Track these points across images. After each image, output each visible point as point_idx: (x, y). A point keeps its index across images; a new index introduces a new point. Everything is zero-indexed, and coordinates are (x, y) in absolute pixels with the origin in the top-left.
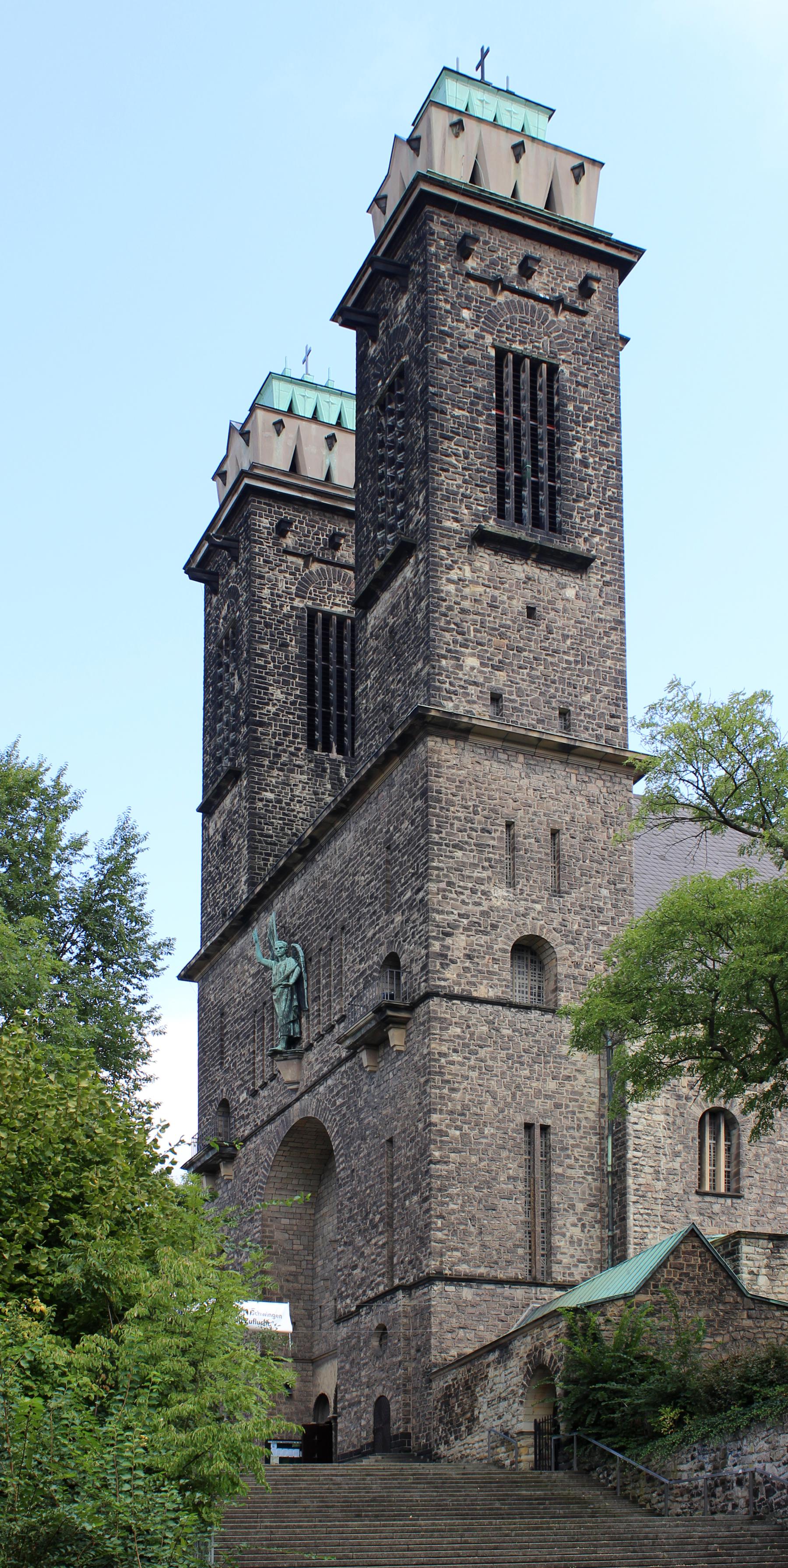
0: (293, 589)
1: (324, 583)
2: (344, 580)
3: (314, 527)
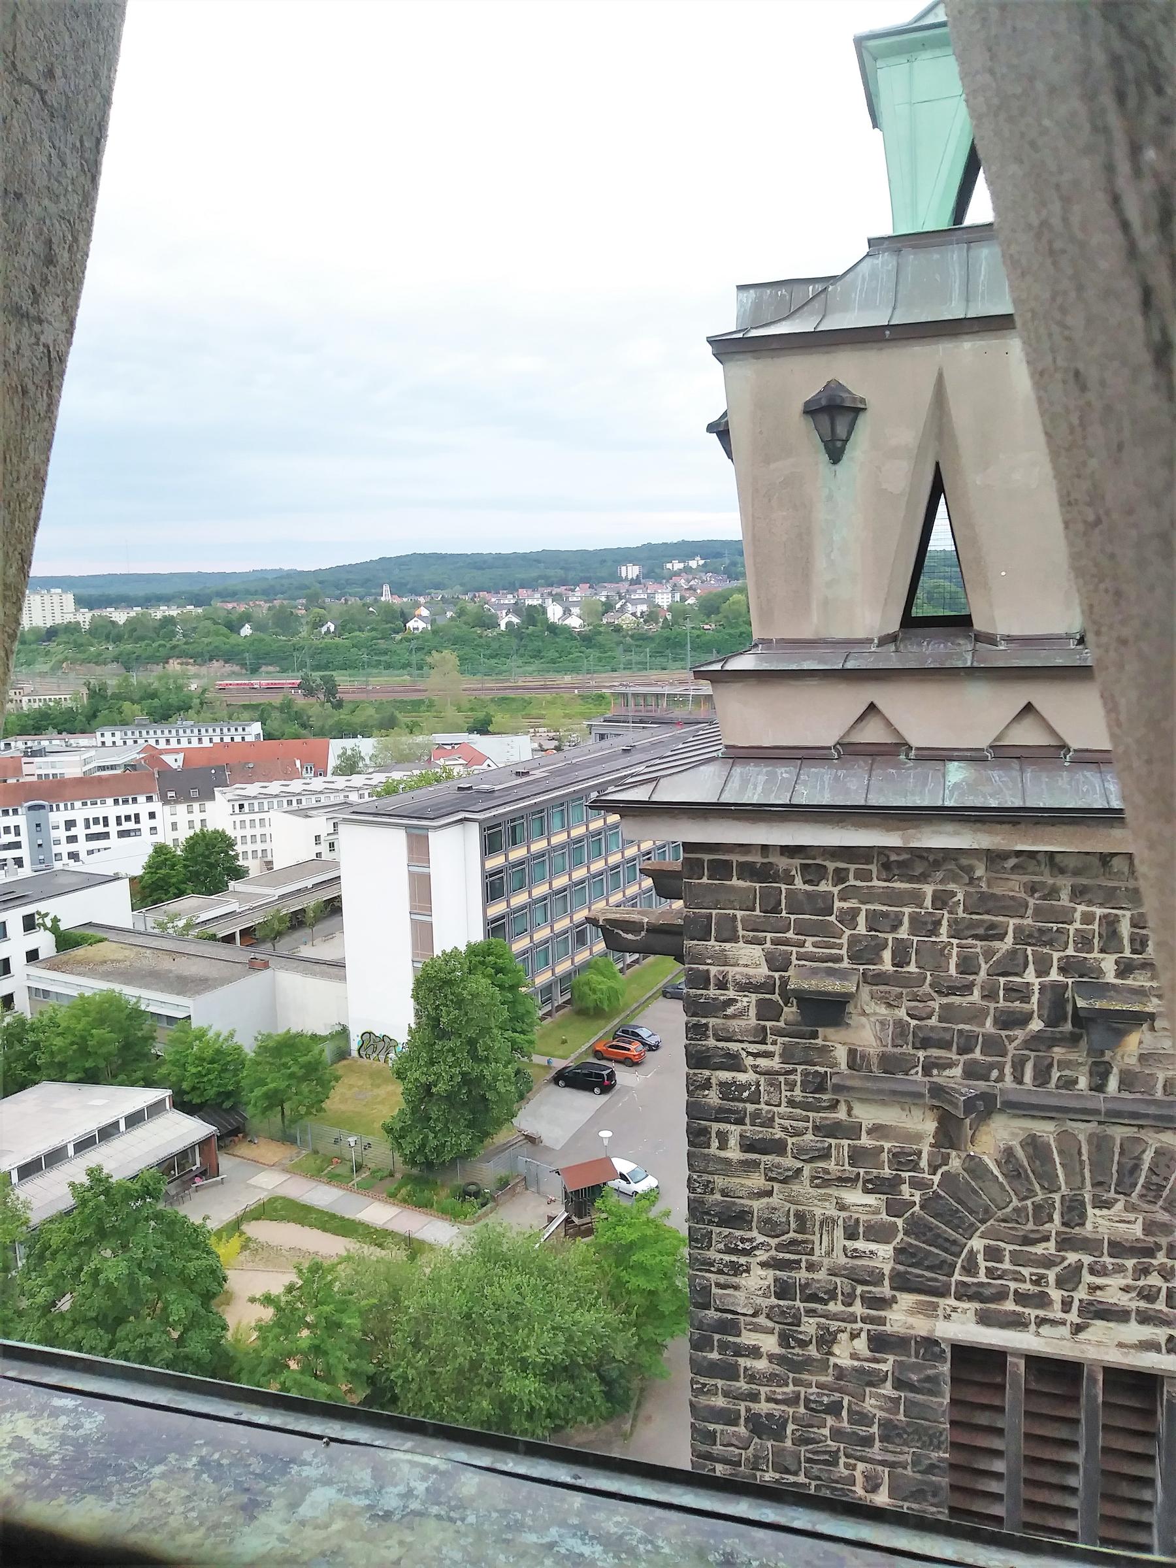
0: (883, 1255)
1: (1042, 1213)
3: (994, 933)
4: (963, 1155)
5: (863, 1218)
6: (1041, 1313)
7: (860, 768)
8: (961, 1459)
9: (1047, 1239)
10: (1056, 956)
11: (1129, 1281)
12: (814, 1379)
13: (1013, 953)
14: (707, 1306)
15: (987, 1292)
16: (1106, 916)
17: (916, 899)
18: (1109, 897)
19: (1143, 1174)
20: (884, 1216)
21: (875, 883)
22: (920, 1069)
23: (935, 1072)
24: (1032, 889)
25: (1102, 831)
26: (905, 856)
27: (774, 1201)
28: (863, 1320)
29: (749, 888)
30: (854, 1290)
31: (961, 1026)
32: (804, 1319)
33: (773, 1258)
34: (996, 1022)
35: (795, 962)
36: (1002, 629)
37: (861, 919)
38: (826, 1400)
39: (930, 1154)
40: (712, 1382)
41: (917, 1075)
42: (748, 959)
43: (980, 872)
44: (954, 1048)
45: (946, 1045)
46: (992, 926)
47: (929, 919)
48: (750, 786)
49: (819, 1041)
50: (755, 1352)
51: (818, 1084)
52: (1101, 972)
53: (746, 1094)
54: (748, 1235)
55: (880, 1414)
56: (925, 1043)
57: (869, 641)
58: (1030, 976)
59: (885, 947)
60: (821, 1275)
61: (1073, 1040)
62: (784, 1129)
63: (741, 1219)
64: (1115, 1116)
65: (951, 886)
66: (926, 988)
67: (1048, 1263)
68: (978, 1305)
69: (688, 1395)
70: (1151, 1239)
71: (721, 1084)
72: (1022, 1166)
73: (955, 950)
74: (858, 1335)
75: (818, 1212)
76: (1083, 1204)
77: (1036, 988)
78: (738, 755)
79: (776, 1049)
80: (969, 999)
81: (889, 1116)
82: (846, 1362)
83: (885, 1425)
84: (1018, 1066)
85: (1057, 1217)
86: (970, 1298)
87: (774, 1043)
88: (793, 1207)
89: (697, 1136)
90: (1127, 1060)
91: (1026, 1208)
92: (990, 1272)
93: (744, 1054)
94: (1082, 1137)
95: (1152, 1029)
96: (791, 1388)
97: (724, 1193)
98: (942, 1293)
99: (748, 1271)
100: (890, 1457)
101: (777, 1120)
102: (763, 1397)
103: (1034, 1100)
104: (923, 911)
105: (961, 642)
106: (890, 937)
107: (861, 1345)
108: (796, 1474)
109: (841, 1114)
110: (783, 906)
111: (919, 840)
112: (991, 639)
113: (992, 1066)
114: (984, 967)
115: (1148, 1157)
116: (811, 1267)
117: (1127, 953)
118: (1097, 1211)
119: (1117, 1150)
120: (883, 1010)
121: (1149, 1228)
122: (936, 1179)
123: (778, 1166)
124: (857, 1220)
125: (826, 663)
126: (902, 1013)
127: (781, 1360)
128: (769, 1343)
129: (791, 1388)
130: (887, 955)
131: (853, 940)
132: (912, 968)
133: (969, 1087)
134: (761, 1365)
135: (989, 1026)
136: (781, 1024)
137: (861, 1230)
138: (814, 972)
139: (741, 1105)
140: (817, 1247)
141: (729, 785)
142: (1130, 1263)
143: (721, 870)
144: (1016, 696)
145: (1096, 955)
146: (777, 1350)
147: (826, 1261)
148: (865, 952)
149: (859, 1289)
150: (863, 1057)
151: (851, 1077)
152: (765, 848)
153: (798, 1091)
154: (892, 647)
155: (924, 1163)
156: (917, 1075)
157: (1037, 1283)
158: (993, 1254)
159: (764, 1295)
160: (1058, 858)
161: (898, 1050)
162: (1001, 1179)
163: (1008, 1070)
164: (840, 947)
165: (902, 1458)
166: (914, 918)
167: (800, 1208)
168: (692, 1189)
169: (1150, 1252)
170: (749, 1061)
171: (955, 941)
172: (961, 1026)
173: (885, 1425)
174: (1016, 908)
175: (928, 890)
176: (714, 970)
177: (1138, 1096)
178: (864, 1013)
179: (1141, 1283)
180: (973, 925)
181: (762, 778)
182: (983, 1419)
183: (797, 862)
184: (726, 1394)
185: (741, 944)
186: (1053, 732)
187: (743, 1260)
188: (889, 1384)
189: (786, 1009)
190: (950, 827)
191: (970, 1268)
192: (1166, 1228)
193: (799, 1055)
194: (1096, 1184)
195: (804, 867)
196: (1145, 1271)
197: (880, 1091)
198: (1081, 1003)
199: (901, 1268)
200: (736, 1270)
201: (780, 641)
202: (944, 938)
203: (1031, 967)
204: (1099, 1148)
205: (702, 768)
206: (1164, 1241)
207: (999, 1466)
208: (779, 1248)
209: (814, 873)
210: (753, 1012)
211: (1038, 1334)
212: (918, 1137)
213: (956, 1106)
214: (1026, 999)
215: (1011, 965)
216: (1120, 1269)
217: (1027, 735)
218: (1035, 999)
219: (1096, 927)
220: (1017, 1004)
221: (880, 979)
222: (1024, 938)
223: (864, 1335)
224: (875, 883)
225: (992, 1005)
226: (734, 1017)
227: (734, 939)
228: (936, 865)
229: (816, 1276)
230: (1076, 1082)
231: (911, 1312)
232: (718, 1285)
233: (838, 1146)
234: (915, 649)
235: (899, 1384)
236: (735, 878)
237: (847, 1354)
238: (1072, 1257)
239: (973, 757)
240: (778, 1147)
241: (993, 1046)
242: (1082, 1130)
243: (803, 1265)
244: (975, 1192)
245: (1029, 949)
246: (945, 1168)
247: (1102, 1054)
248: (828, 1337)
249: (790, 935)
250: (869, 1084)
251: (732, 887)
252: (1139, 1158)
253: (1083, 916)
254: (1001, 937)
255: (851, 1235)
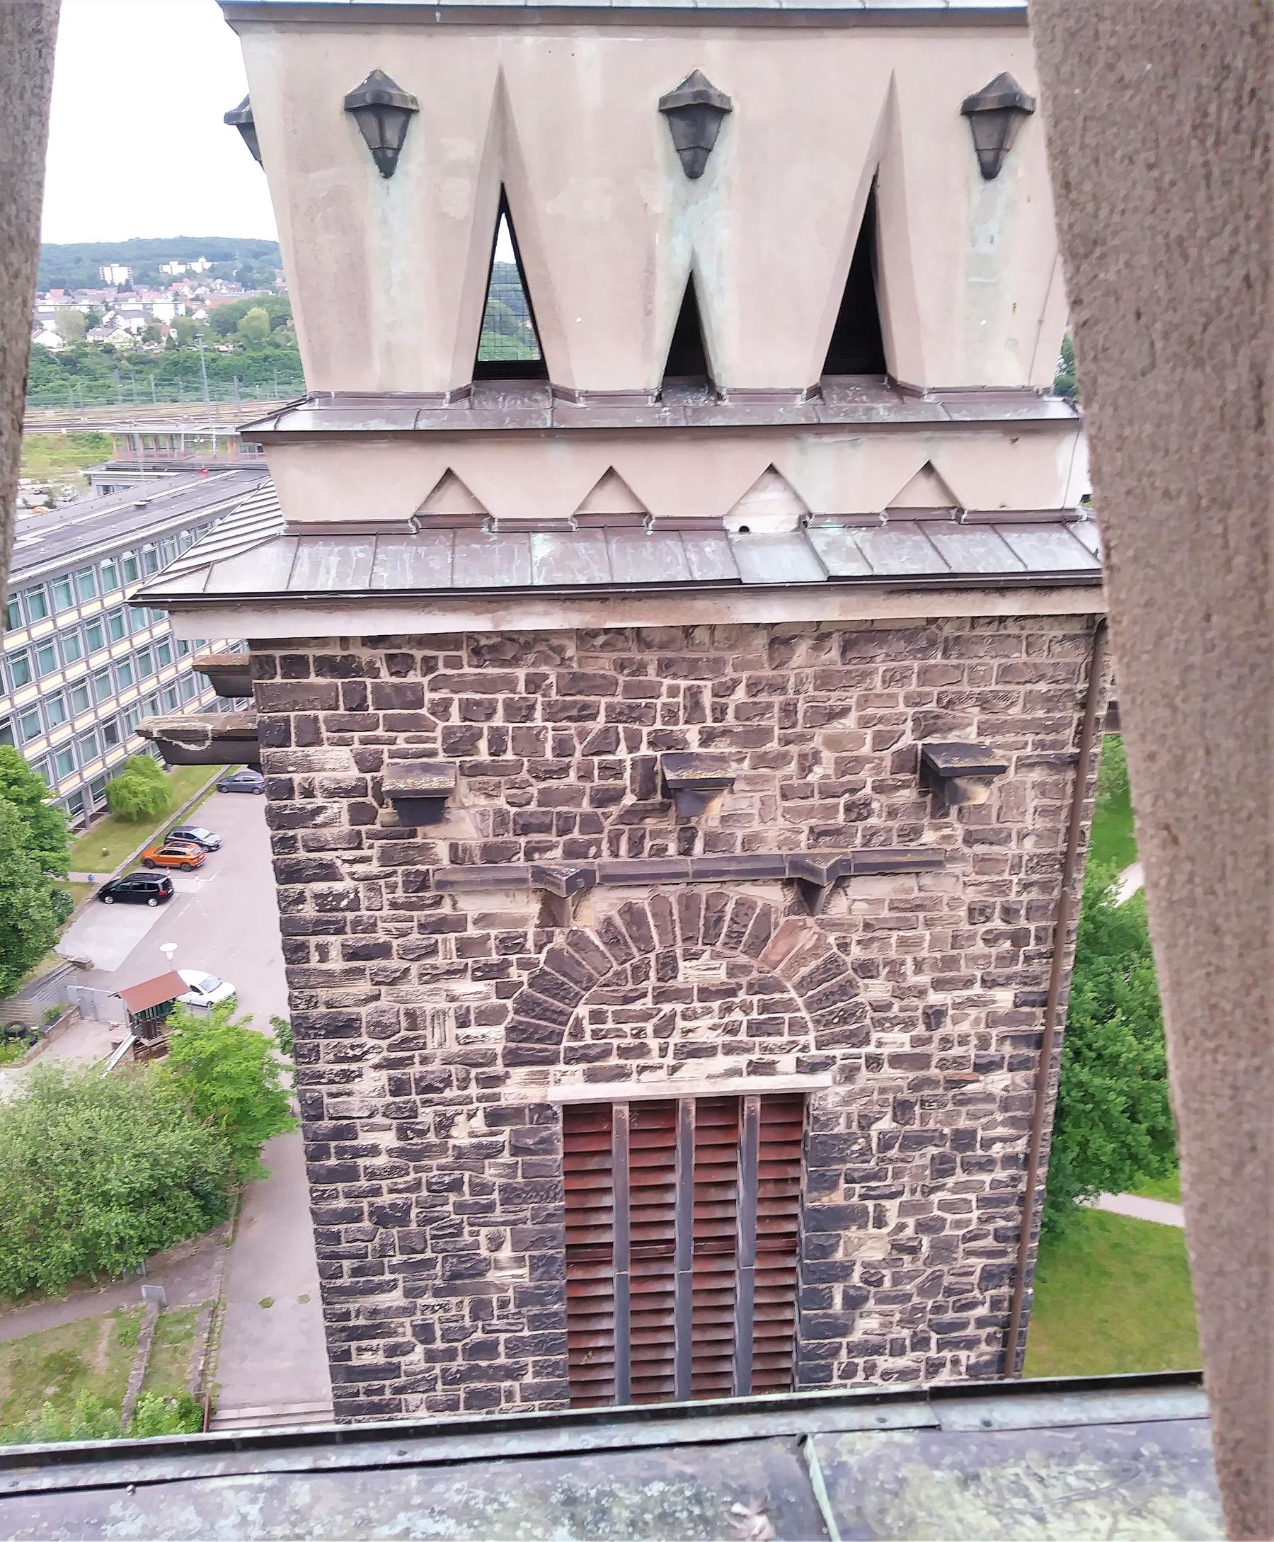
0: (495, 1037)
1: (639, 973)
2: (735, 937)
3: (586, 713)
4: (567, 931)
5: (473, 1005)
6: (641, 1062)
7: (442, 542)
8: (576, 1202)
9: (644, 995)
10: (645, 731)
11: (716, 1021)
12: (434, 1163)
13: (607, 730)
14: (320, 1118)
15: (593, 1052)
16: (689, 688)
17: (510, 684)
18: (693, 669)
19: (726, 924)
20: (494, 1001)
21: (467, 670)
22: (521, 855)
23: (536, 856)
24: (621, 666)
25: (687, 603)
26: (495, 640)
27: (383, 1003)
28: (479, 1100)
29: (328, 686)
30: (468, 1073)
31: (559, 809)
32: (421, 1110)
33: (385, 1059)
34: (592, 801)
35: (387, 760)
36: (580, 385)
37: (455, 710)
38: (447, 1179)
39: (536, 935)
40: (332, 1187)
41: (520, 861)
42: (336, 762)
43: (570, 653)
44: (554, 830)
45: (545, 829)
46: (585, 706)
47: (523, 704)
48: (322, 570)
49: (419, 840)
50: (374, 1151)
51: (421, 882)
52: (686, 743)
53: (344, 903)
54: (357, 1041)
55: (499, 1181)
56: (525, 830)
57: (440, 396)
58: (622, 753)
59: (480, 736)
60: (436, 1066)
61: (663, 810)
62: (389, 932)
63: (348, 1027)
64: (701, 875)
65: (544, 669)
66: (524, 775)
67: (646, 1016)
68: (585, 1066)
69: (307, 1202)
70: (733, 981)
71: (316, 896)
72: (620, 933)
73: (550, 734)
74: (474, 1115)
75: (428, 1007)
76: (675, 958)
77: (628, 764)
78: (305, 533)
79: (374, 853)
80: (566, 781)
81: (494, 904)
82: (465, 1141)
83: (503, 1189)
84: (614, 839)
85: (652, 974)
86: (578, 1060)
87: (371, 847)
88: (402, 1007)
89: (294, 953)
90: (711, 823)
91: (625, 970)
92: (595, 1034)
93: (339, 863)
94: (673, 899)
95: (732, 792)
96: (412, 1175)
97: (329, 1005)
98: (552, 1061)
99: (360, 1076)
100: (511, 1217)
101: (380, 924)
102: (385, 1190)
103: (630, 871)
104: (517, 697)
105: (538, 397)
106: (485, 726)
107: (479, 1123)
108: (422, 1252)
109: (446, 909)
110: (370, 701)
111: (510, 622)
112: (569, 395)
113: (589, 844)
114: (579, 748)
115: (729, 909)
116: (424, 1060)
117: (709, 723)
118: (687, 964)
119: (703, 906)
120: (482, 801)
121: (731, 972)
122: (542, 957)
123: (384, 970)
124: (468, 1009)
125: (394, 422)
126: (501, 802)
127: (401, 1152)
128: (388, 1140)
129: (412, 1175)
130: (483, 745)
131: (448, 732)
132: (509, 756)
133: (569, 866)
134: (381, 1161)
135: (586, 806)
136: (377, 827)
137: (472, 1017)
138: (409, 769)
139: (340, 915)
140: (429, 1040)
141: (298, 569)
142: (716, 1005)
143: (296, 666)
144: (600, 458)
145: (681, 726)
146: (397, 1144)
147: (439, 1052)
148: (460, 744)
149: (474, 1072)
150: (464, 850)
151: (453, 871)
152: (344, 641)
153: (400, 895)
154: (466, 403)
155: (530, 944)
156: (520, 861)
157: (637, 1036)
158: (597, 1017)
159: (379, 1096)
160: (644, 634)
161: (500, 839)
162: (602, 947)
163: (605, 846)
164: (434, 740)
165: (521, 1215)
166: (508, 705)
167: (410, 1006)
168: (295, 1007)
169: (732, 992)
170: (345, 869)
171: (550, 725)
172: (559, 809)
173: (503, 1189)
174: (605, 686)
175: (521, 673)
176: (297, 778)
177: (720, 855)
178: (463, 807)
179: (725, 1020)
180: (566, 707)
181: (334, 560)
182: (593, 1164)
183: (382, 652)
184: (347, 1195)
185: (326, 747)
186: (635, 499)
187: (354, 1066)
188: (506, 1152)
189: (381, 811)
190: (540, 607)
191: (577, 1034)
192: (746, 969)
193: (399, 857)
194: (686, 939)
195: (390, 658)
196: (729, 1009)
197: (483, 882)
198: (670, 776)
199: (513, 1045)
200: (348, 1076)
201: (338, 394)
202: (539, 722)
203: (623, 745)
204: (687, 907)
205: (262, 549)
206: (744, 980)
207: (608, 1201)
208: (391, 1048)
209: (400, 664)
210: (345, 817)
211: (639, 1081)
212: (523, 921)
213: (558, 886)
214: (618, 775)
215: (605, 743)
216: (708, 1011)
217: (610, 503)
218: (627, 775)
219: (680, 699)
220: (611, 781)
221: (476, 770)
222: (616, 715)
223: (480, 1114)
224: (467, 670)
225: (588, 785)
226: (324, 825)
227: (318, 742)
228: (527, 647)
229: (429, 1068)
230: (666, 849)
231: (525, 1083)
232: (331, 1095)
233: (445, 941)
234: (490, 405)
235: (516, 1151)
236: (313, 675)
237: (465, 1134)
238: (666, 1008)
239: (558, 528)
240: (383, 951)
241: (591, 824)
242: (672, 893)
243: (417, 1060)
244: (579, 964)
245: (621, 726)
246: (549, 946)
247: (689, 821)
248: (446, 1123)
249: (380, 732)
250: (473, 877)
251: (310, 687)
252: (722, 911)
253: (669, 689)
254: (594, 717)
255: (463, 1024)
